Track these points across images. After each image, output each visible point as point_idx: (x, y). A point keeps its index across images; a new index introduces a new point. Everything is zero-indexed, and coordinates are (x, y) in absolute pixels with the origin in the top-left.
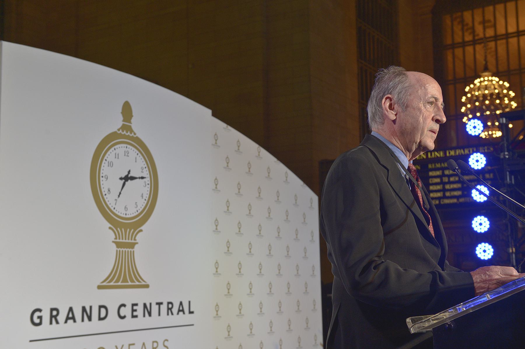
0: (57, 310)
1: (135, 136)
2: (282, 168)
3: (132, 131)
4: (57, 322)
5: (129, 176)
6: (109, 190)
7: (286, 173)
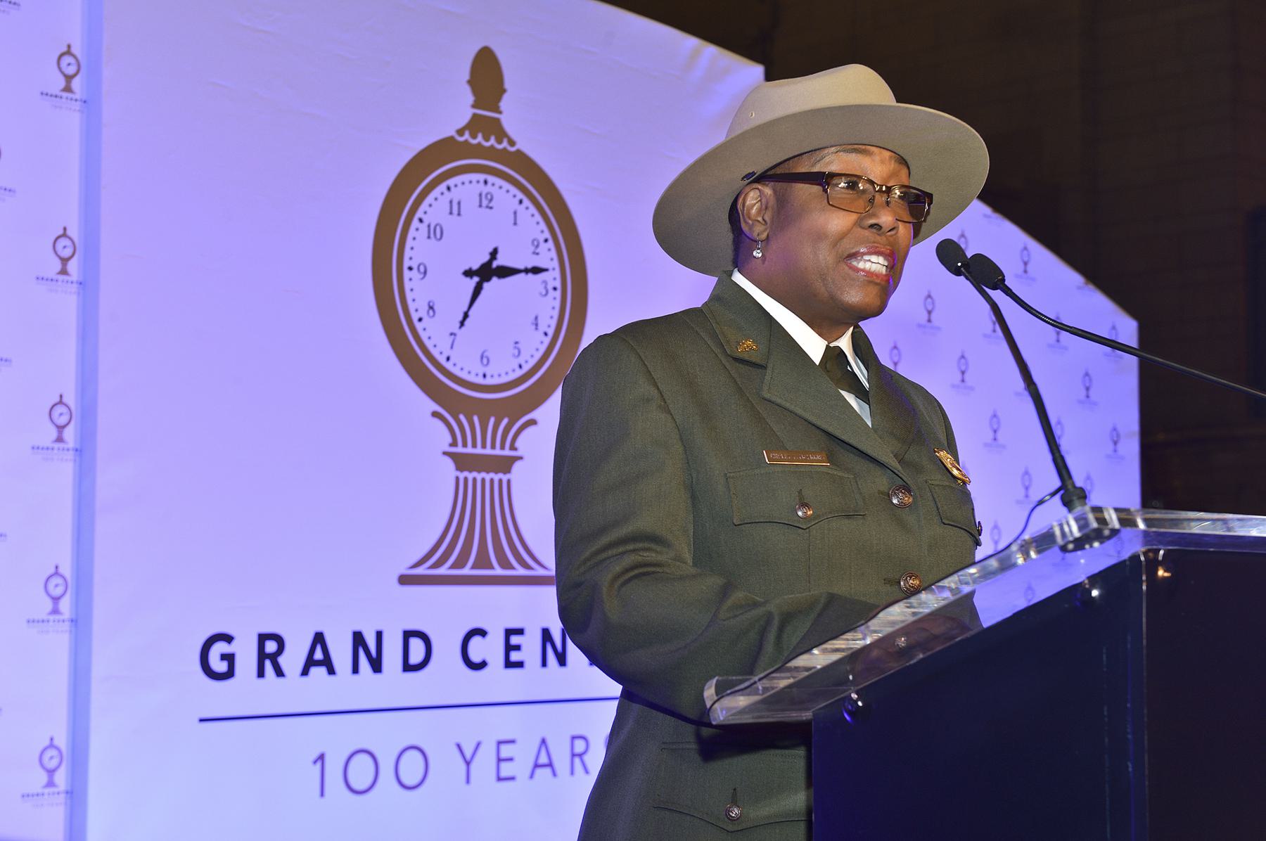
0: (279, 639)
1: (513, 149)
3: (501, 134)
4: (279, 672)
5: (495, 264)
6: (431, 308)
7: (1025, 248)
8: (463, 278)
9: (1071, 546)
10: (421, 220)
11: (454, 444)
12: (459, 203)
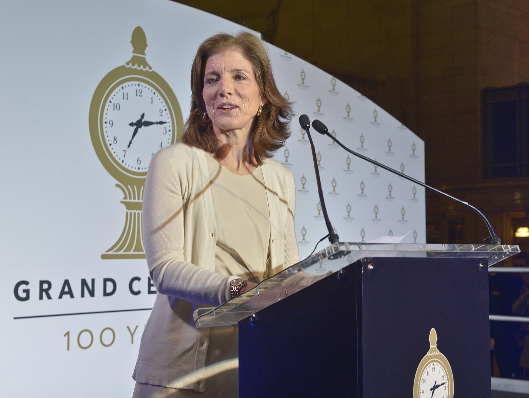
1: (151, 71)
2: (369, 106)
3: (146, 64)
4: (49, 297)
5: (143, 120)
6: (115, 139)
7: (375, 111)
8: (129, 126)
9: (332, 257)
10: (110, 102)
11: (125, 198)
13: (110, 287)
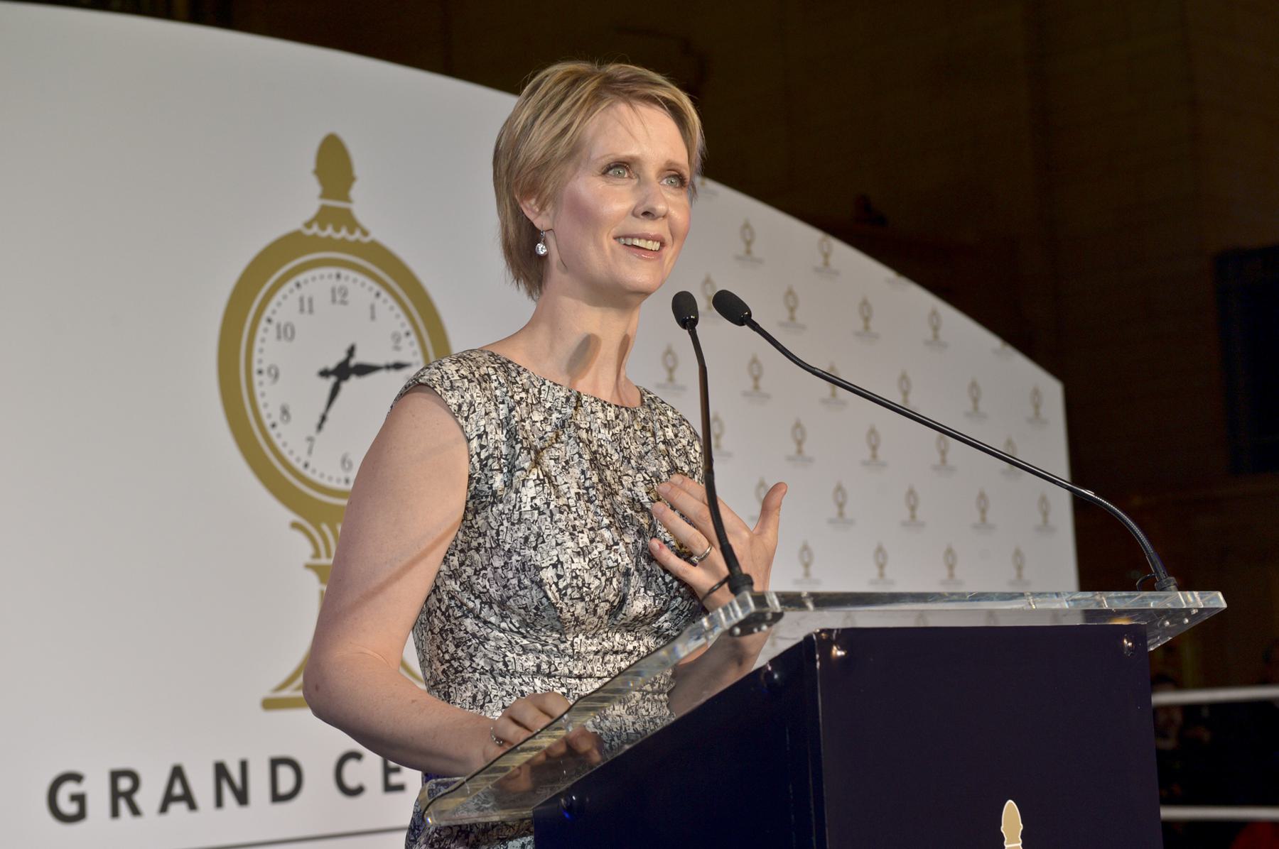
1: (366, 240)
3: (353, 225)
4: (135, 811)
5: (353, 362)
6: (285, 412)
9: (737, 631)
10: (269, 321)
11: (317, 555)
12: (311, 301)
13: (286, 779)
